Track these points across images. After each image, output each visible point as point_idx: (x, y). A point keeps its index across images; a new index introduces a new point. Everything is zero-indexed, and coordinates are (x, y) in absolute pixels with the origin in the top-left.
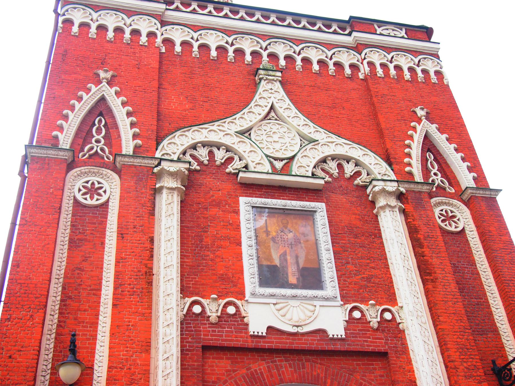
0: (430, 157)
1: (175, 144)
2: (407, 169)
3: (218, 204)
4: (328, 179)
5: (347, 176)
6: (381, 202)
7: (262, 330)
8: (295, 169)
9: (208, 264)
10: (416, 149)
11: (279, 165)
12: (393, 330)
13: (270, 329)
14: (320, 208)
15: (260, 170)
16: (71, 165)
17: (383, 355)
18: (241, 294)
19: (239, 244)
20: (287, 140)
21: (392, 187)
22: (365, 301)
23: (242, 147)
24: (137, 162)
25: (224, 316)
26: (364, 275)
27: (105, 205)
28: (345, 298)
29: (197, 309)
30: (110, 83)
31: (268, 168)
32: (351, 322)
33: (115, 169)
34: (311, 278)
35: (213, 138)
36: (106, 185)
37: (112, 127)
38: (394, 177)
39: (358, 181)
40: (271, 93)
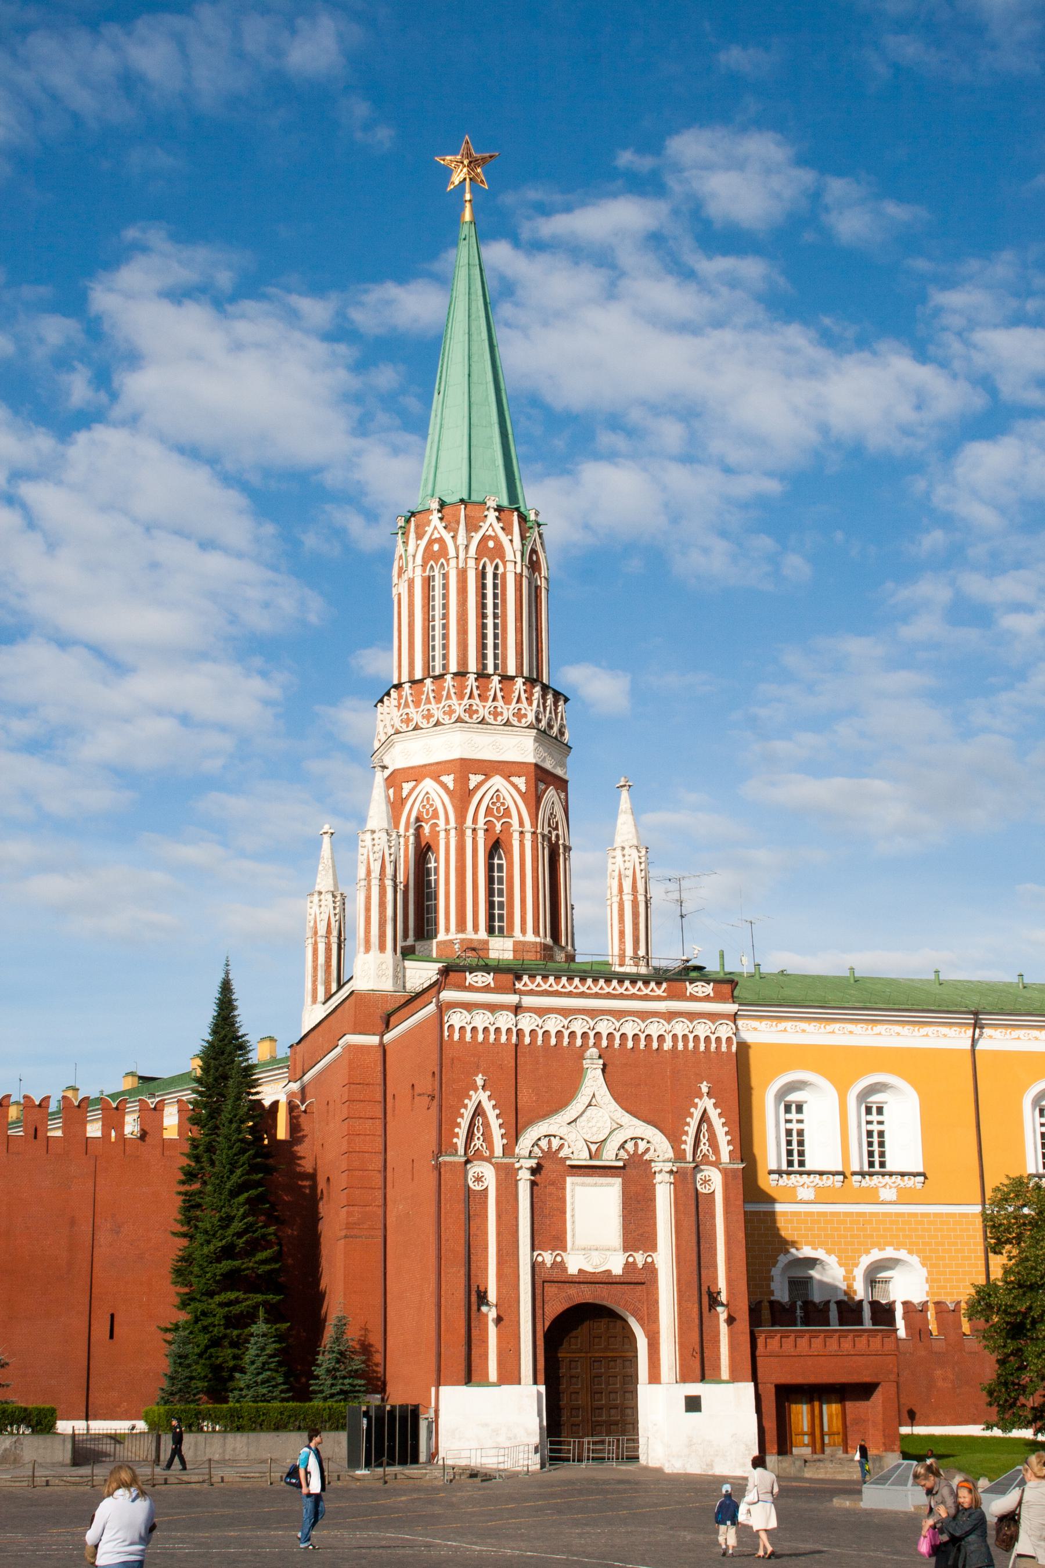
2: (683, 1146)
3: (553, 1183)
5: (640, 1152)
6: (659, 1178)
7: (575, 1272)
8: (604, 1157)
10: (693, 1123)
11: (593, 1148)
12: (651, 1269)
13: (580, 1271)
15: (581, 1157)
18: (564, 1249)
19: (565, 1213)
21: (668, 1166)
22: (636, 1251)
25: (554, 1263)
32: (627, 1263)
33: (491, 1163)
36: (486, 1175)
37: (487, 1125)
39: (647, 1157)
40: (594, 1082)
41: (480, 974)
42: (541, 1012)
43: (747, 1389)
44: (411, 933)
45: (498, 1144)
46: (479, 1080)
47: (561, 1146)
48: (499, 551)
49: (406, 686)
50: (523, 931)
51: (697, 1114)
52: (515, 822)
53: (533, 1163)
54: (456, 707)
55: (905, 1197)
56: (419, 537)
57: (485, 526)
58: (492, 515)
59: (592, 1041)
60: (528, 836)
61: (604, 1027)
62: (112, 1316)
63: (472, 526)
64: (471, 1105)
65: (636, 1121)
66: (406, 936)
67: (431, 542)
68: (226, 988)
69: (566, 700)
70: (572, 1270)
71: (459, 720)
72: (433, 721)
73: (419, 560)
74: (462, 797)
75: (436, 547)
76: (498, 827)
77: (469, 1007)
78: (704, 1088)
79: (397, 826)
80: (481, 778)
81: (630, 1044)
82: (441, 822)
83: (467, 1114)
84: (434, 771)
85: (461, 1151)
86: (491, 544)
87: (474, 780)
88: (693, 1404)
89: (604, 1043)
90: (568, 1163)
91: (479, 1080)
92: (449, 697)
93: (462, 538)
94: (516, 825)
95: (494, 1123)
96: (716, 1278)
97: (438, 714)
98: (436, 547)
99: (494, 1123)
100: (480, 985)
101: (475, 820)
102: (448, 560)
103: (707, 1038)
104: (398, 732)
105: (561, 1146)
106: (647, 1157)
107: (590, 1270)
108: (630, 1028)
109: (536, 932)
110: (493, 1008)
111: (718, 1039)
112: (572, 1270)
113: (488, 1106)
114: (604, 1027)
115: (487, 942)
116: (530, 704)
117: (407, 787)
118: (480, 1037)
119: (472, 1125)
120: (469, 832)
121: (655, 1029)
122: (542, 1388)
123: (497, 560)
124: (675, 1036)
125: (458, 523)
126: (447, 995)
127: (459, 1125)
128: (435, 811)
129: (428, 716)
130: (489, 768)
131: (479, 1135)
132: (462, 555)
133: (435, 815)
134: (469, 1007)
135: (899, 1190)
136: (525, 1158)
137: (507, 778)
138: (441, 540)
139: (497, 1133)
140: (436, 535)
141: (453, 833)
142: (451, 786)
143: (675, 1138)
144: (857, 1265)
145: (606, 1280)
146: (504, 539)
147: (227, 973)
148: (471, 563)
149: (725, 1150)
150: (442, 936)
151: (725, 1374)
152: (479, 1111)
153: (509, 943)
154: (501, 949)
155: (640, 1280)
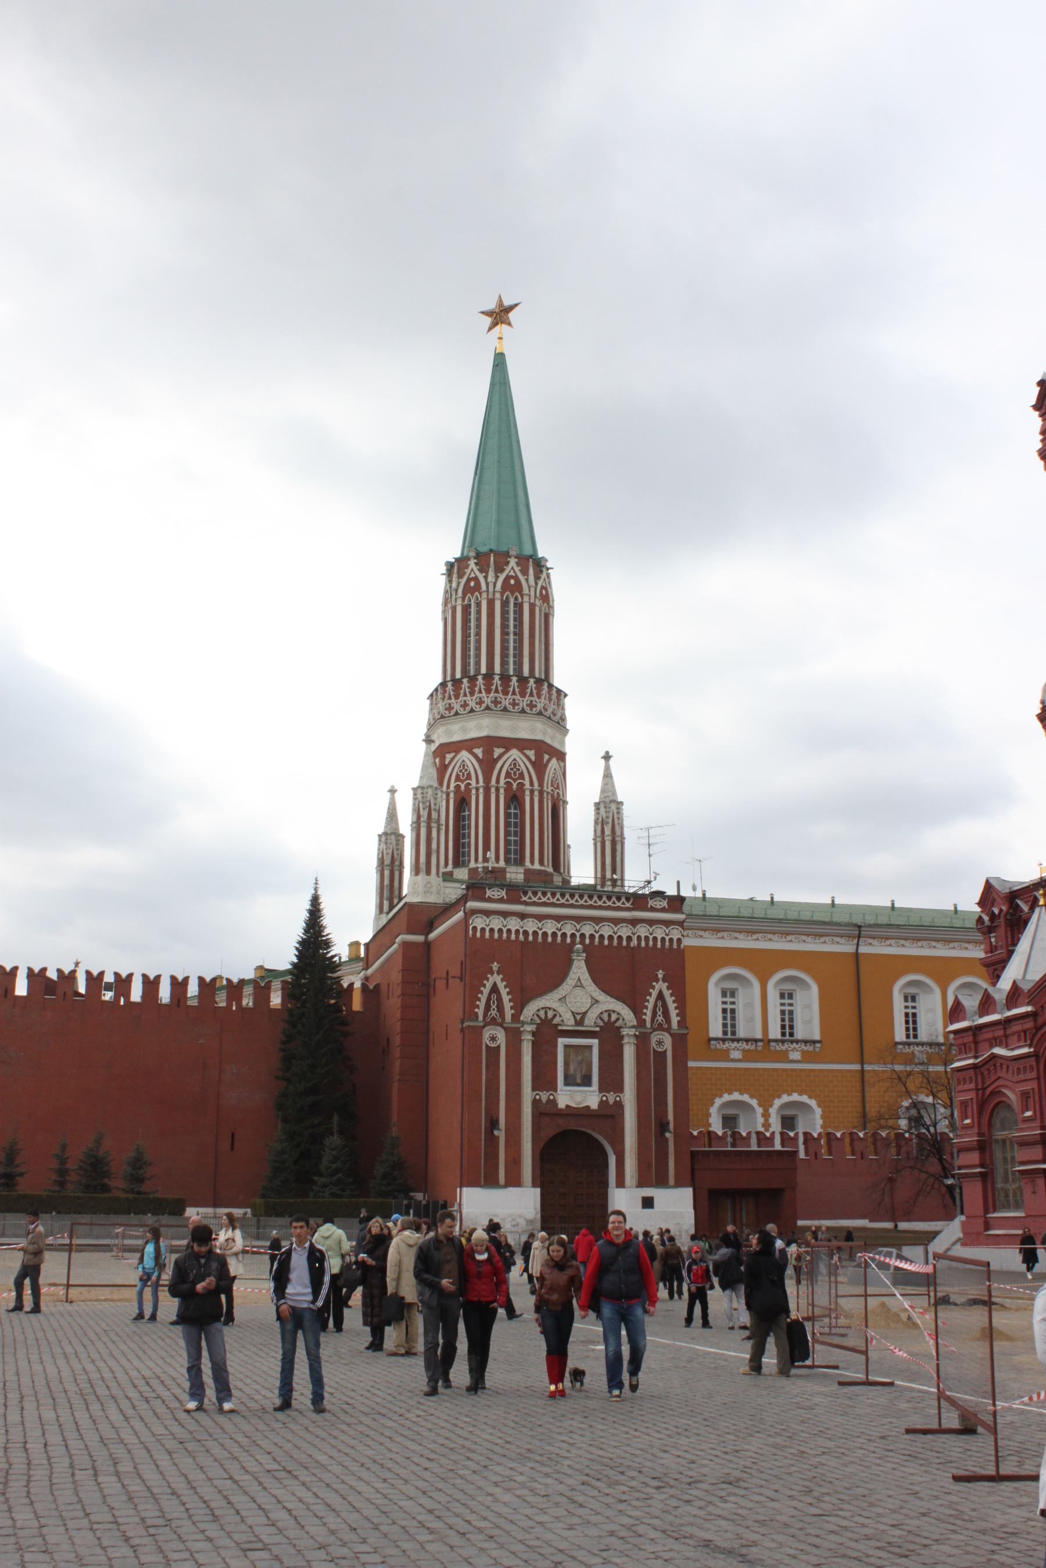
0: (660, 1003)
1: (530, 1010)
4: (602, 1024)
6: (626, 1040)
8: (586, 1022)
9: (544, 1079)
10: (652, 1000)
11: (578, 1017)
12: (619, 1105)
13: (567, 1106)
14: (595, 1042)
15: (569, 1023)
16: (484, 1027)
17: (612, 1116)
18: (556, 1090)
20: (584, 1000)
21: (632, 1032)
22: (609, 1092)
23: (561, 1010)
24: (513, 1025)
25: (549, 1099)
26: (612, 1081)
27: (499, 1046)
28: (601, 1090)
29: (538, 1097)
30: (498, 974)
31: (572, 1022)
32: (603, 1104)
33: (502, 1027)
34: (587, 1081)
35: (548, 1004)
37: (500, 1000)
38: (635, 1023)
39: (617, 1024)
40: (579, 969)
41: (496, 889)
42: (540, 918)
43: (688, 1193)
44: (450, 862)
45: (509, 1013)
46: (495, 966)
47: (555, 1016)
48: (518, 586)
49: (449, 684)
50: (532, 862)
51: (654, 994)
52: (527, 782)
53: (533, 1028)
54: (486, 699)
55: (806, 1057)
56: (460, 576)
57: (508, 569)
58: (513, 562)
59: (578, 939)
60: (536, 793)
61: (588, 929)
62: (233, 1135)
63: (499, 569)
64: (489, 985)
65: (609, 999)
66: (446, 864)
67: (469, 580)
68: (315, 901)
69: (566, 695)
70: (562, 1105)
71: (488, 708)
72: (468, 709)
73: (460, 593)
74: (488, 764)
75: (472, 584)
76: (515, 786)
77: (487, 913)
78: (660, 974)
79: (441, 783)
80: (501, 750)
81: (606, 942)
82: (473, 782)
83: (486, 991)
84: (468, 745)
85: (481, 1018)
86: (512, 582)
87: (497, 752)
88: (648, 1203)
89: (587, 941)
90: (560, 1028)
91: (495, 966)
92: (480, 692)
93: (491, 578)
94: (527, 786)
95: (506, 998)
96: (666, 1112)
97: (472, 704)
98: (472, 584)
99: (506, 998)
100: (496, 897)
101: (498, 781)
102: (481, 594)
103: (663, 939)
104: (442, 717)
105: (555, 1016)
106: (617, 1024)
107: (574, 1106)
108: (606, 931)
109: (541, 862)
110: (505, 914)
111: (671, 940)
112: (562, 1105)
113: (501, 986)
114: (588, 929)
115: (503, 871)
116: (539, 696)
117: (449, 757)
118: (496, 936)
119: (489, 999)
120: (493, 790)
121: (625, 931)
122: (538, 1190)
123: (517, 594)
124: (639, 937)
125: (488, 566)
126: (471, 904)
127: (479, 999)
128: (469, 775)
129: (465, 705)
130: (508, 744)
131: (494, 1007)
132: (491, 589)
133: (469, 777)
134: (487, 913)
135: (803, 1053)
136: (527, 1023)
137: (521, 750)
138: (476, 579)
139: (507, 1005)
140: (473, 575)
141: (481, 790)
142: (480, 756)
143: (637, 1009)
144: (771, 1106)
145: (585, 1113)
146: (522, 578)
147: (316, 889)
148: (498, 595)
149: (675, 1020)
150: (472, 865)
151: (672, 1181)
152: (495, 989)
153: (521, 870)
154: (515, 875)
155: (609, 1116)
